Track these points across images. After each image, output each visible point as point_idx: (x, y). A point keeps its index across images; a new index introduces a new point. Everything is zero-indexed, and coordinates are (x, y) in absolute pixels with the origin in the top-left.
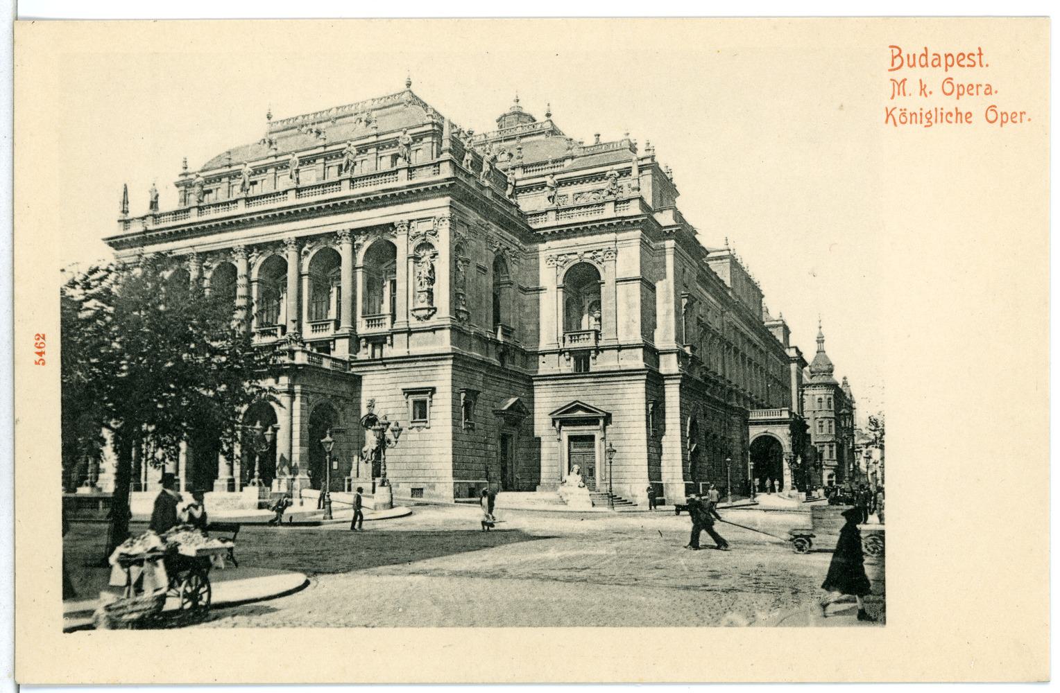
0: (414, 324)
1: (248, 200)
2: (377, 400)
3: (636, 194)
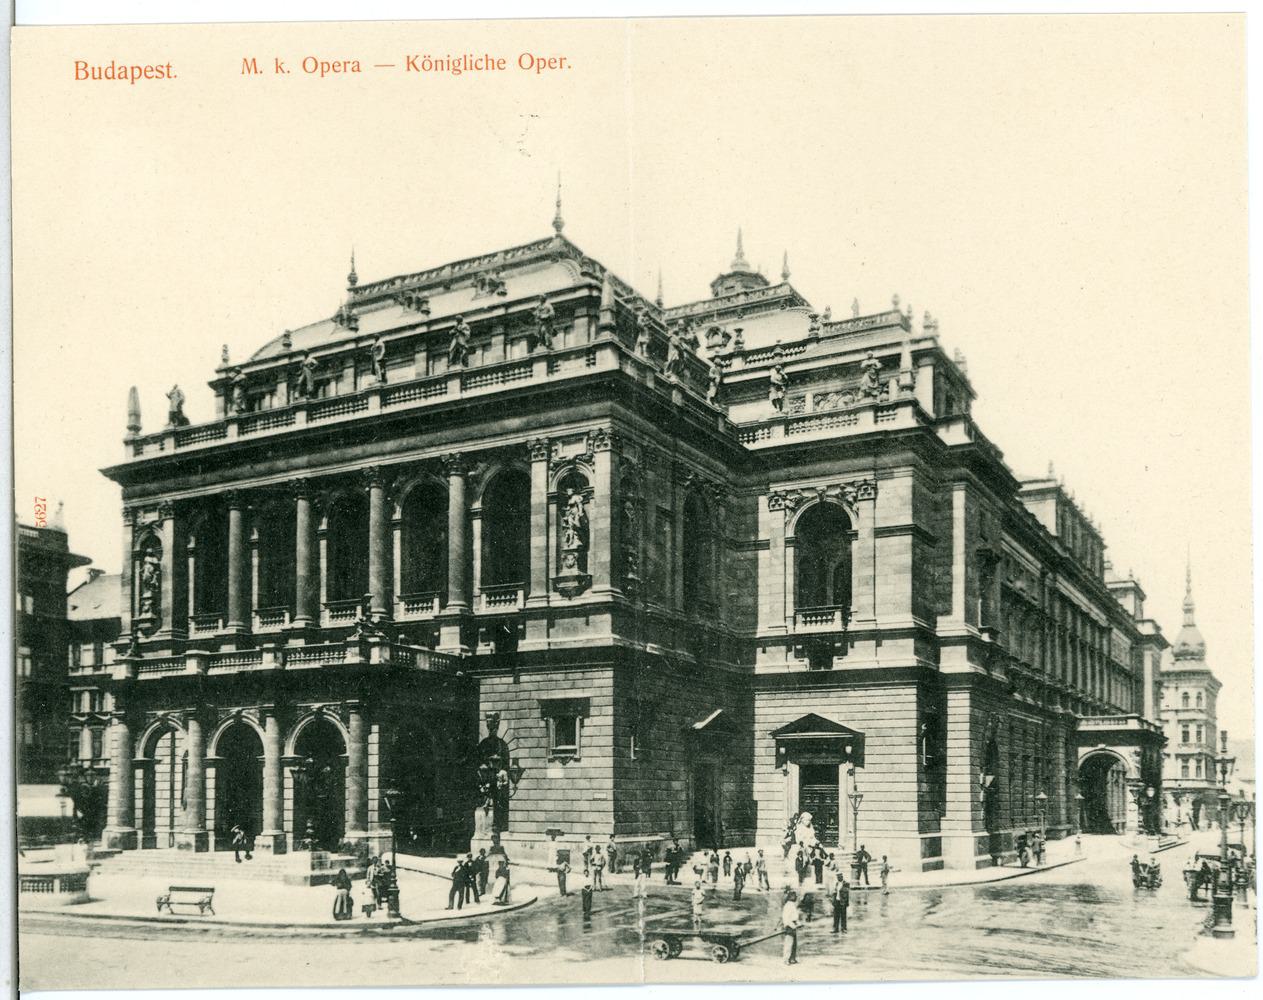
3: (907, 395)
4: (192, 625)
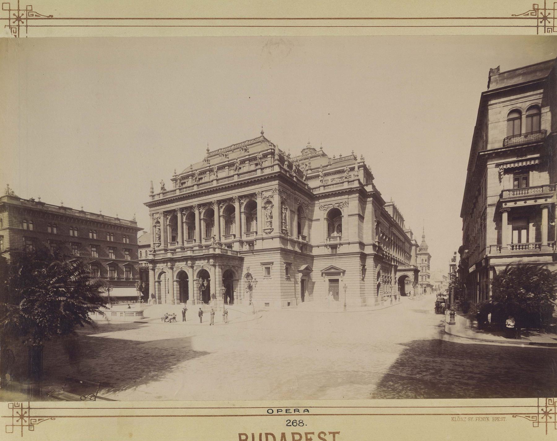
0: (265, 236)
2: (251, 267)
3: (357, 178)
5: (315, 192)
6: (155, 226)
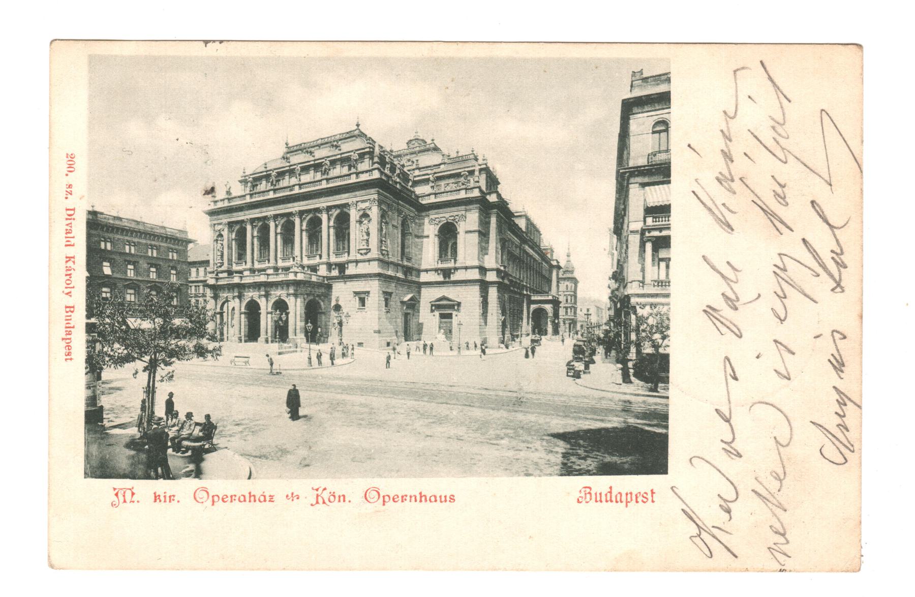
0: (359, 257)
1: (275, 191)
4: (234, 265)
5: (424, 201)
6: (217, 240)
